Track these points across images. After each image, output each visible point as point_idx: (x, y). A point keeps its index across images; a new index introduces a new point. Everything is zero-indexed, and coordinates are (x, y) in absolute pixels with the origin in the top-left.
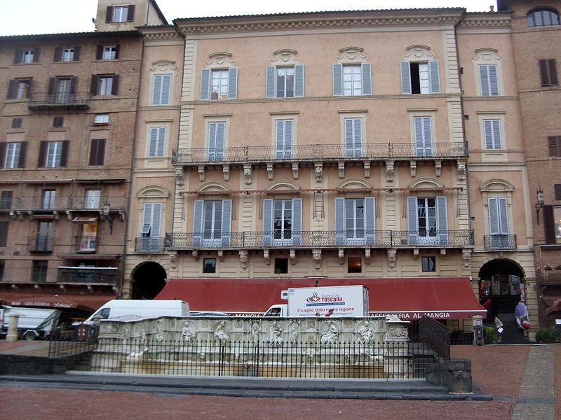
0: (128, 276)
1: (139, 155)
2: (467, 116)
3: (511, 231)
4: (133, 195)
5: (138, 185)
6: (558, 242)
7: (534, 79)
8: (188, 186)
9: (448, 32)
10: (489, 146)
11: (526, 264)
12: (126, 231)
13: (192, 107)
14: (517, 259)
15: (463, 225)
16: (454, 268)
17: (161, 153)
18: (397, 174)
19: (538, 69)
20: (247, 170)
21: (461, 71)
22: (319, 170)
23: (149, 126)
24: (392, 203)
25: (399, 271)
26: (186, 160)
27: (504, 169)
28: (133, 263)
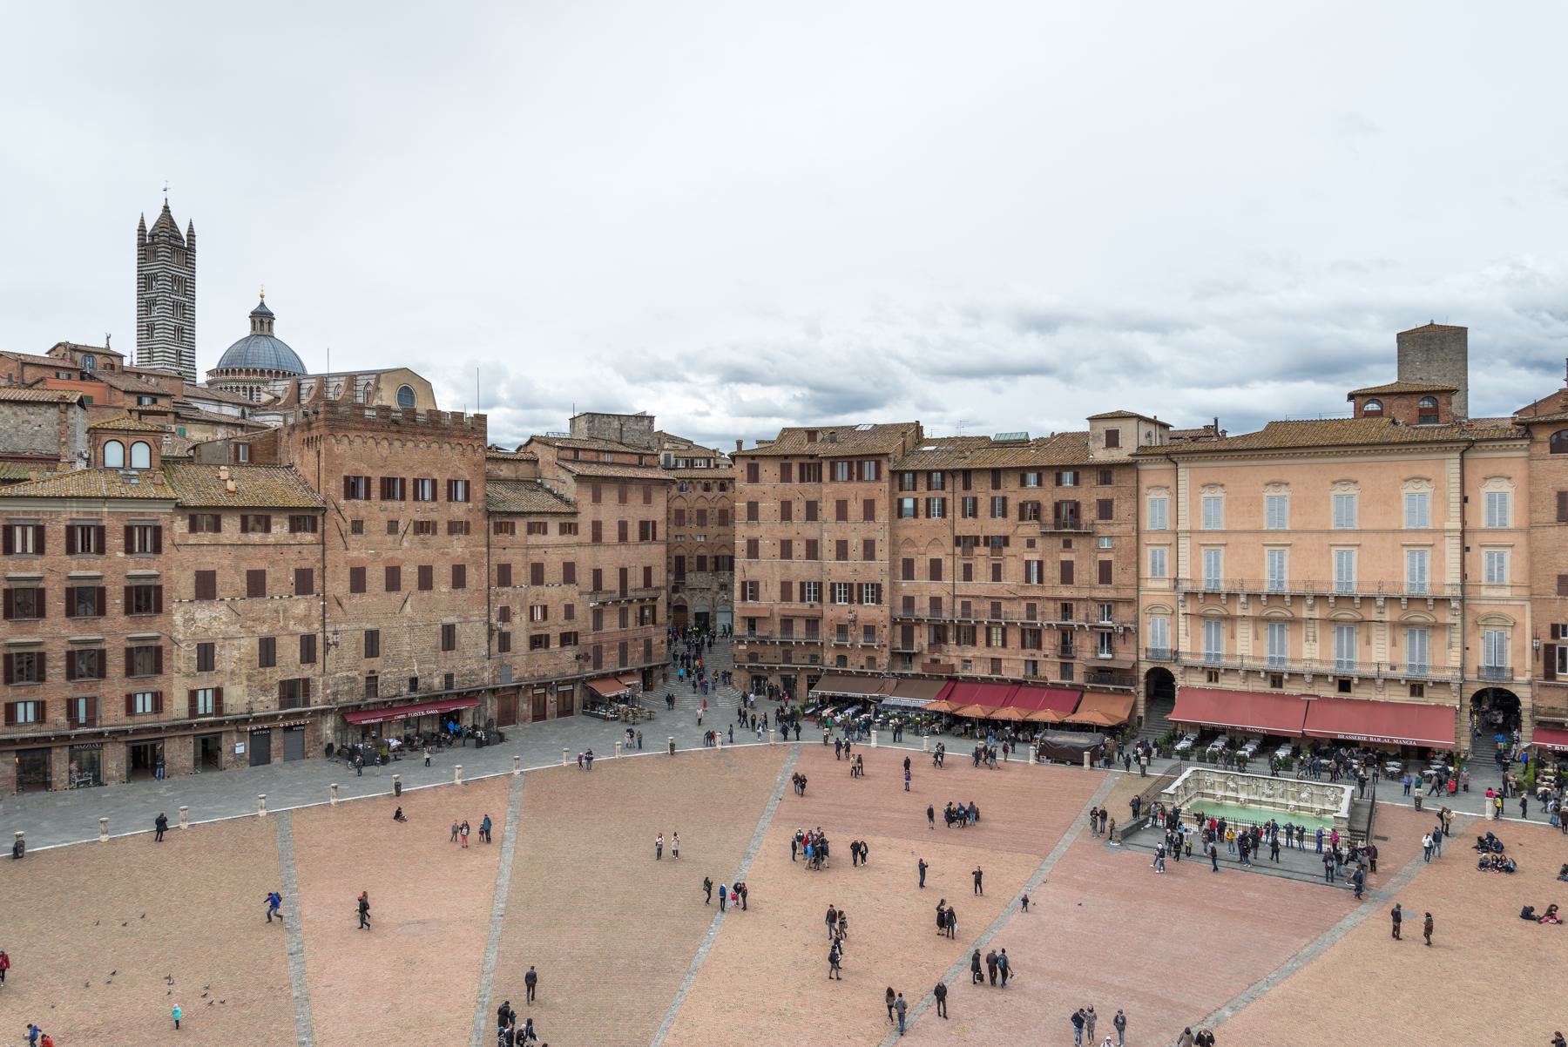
0: (1142, 678)
1: (1143, 575)
3: (1509, 665)
6: (1558, 679)
10: (1491, 578)
11: (1525, 696)
12: (1138, 641)
13: (1188, 535)
14: (1513, 689)
15: (1454, 659)
16: (1442, 696)
17: (1162, 573)
19: (1555, 502)
20: (1243, 599)
21: (1465, 500)
22: (1310, 602)
23: (1149, 548)
25: (1387, 694)
26: (1186, 586)
28: (1145, 667)
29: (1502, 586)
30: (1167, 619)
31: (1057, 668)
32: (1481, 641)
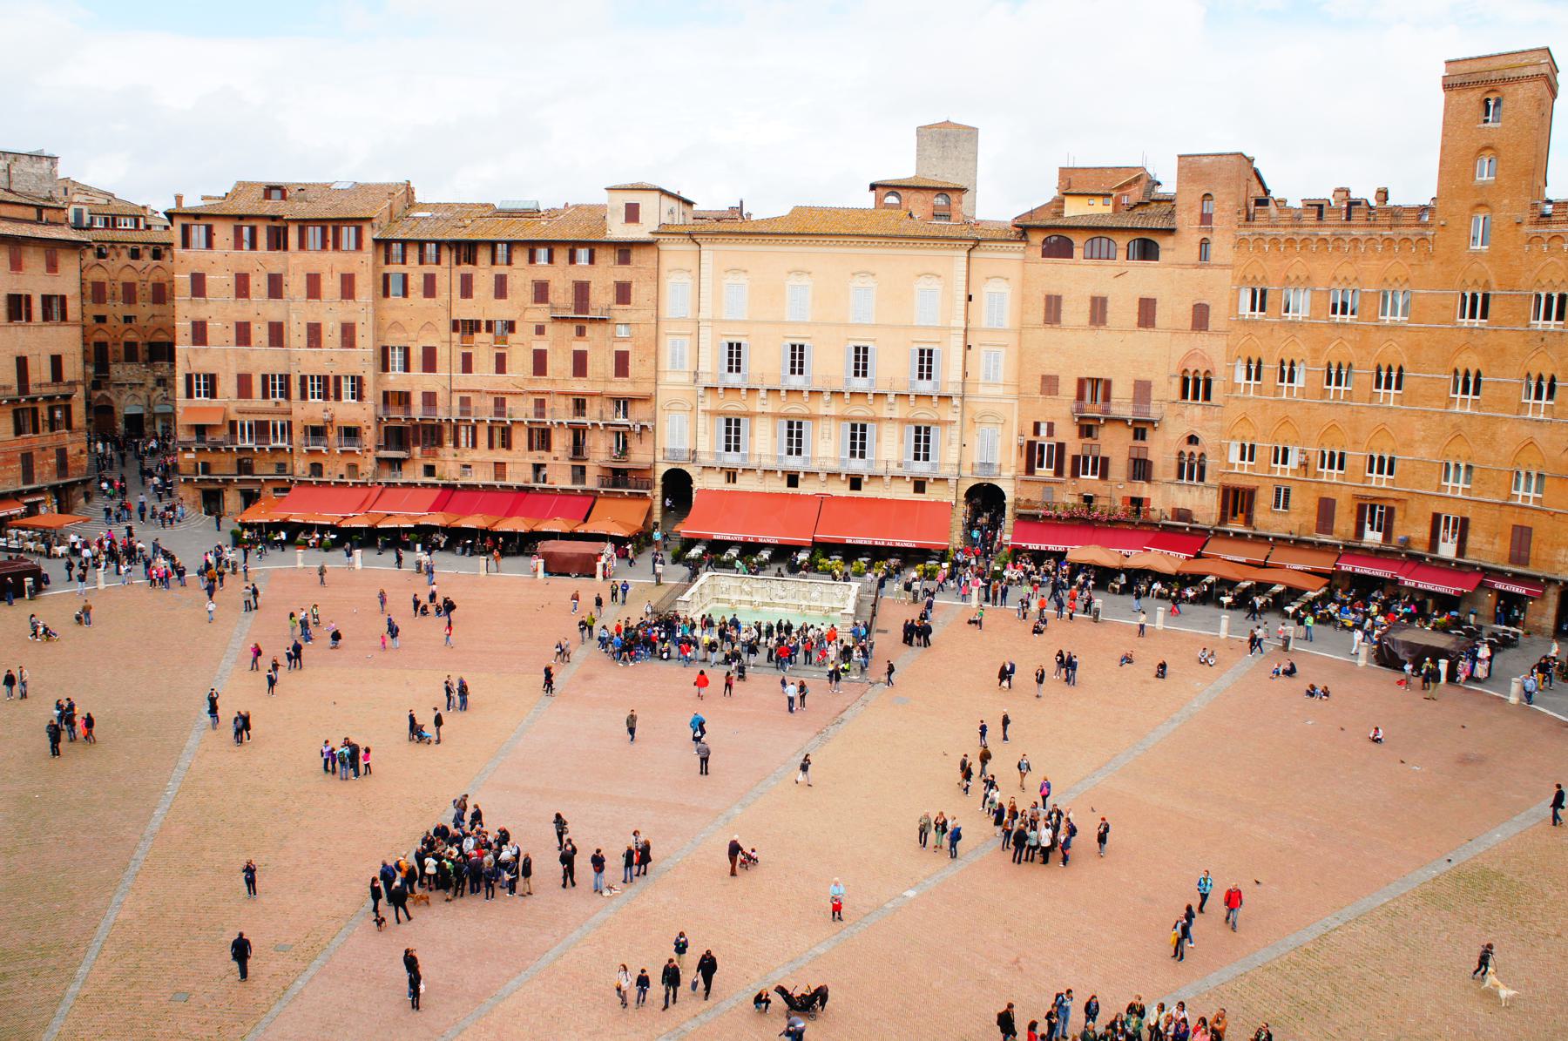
0: (659, 481)
2: (970, 347)
4: (658, 408)
5: (661, 399)
7: (1039, 313)
8: (709, 403)
9: (960, 259)
10: (987, 377)
12: (655, 441)
13: (710, 324)
14: (1000, 484)
15: (953, 457)
17: (682, 366)
18: (898, 404)
19: (1042, 304)
21: (970, 298)
23: (669, 337)
24: (892, 430)
27: (998, 401)
28: (662, 469)
29: (996, 385)
30: (685, 416)
31: (569, 471)
32: (976, 437)
